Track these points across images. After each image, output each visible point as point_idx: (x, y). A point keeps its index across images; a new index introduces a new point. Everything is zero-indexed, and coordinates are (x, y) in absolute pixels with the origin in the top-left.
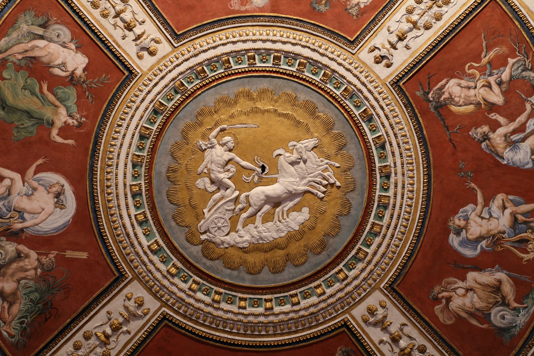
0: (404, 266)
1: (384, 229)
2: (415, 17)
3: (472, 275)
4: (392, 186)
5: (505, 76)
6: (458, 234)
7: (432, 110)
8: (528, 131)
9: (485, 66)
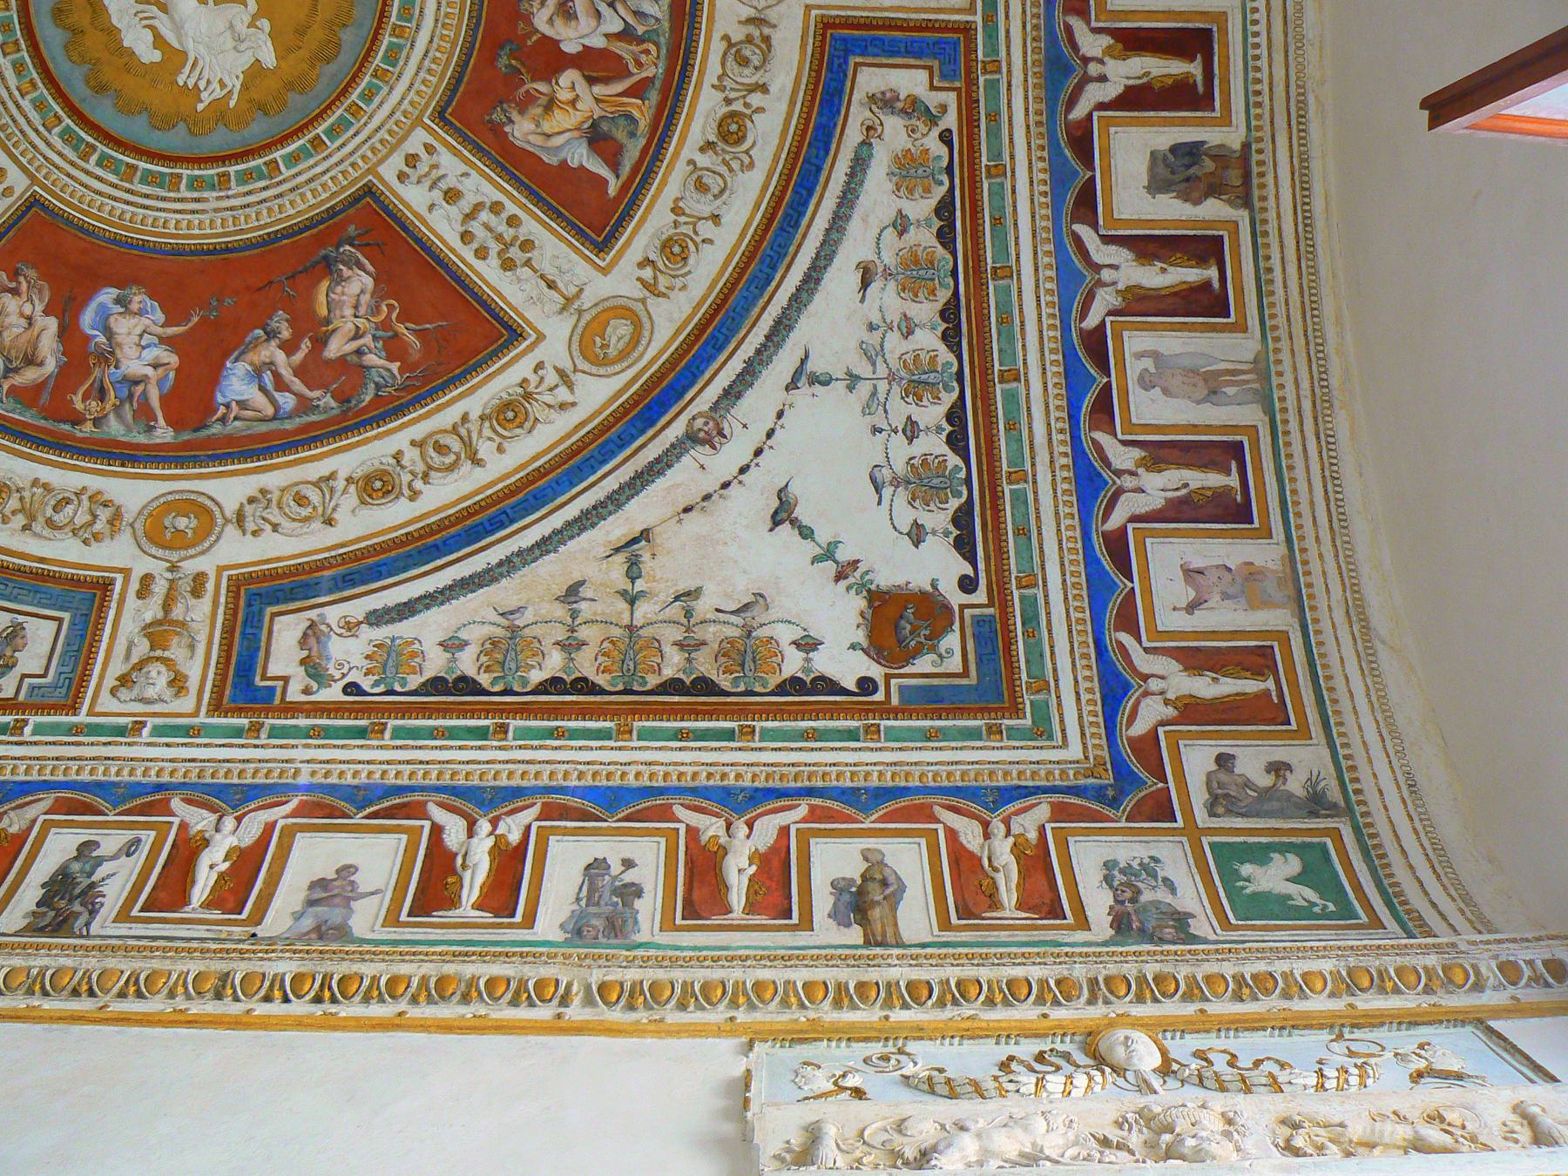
0: (69, 221)
1: (127, 185)
2: (484, 216)
3: (52, 323)
4: (196, 195)
5: (371, 359)
6: (118, 301)
7: (323, 252)
8: (277, 395)
9: (391, 328)
